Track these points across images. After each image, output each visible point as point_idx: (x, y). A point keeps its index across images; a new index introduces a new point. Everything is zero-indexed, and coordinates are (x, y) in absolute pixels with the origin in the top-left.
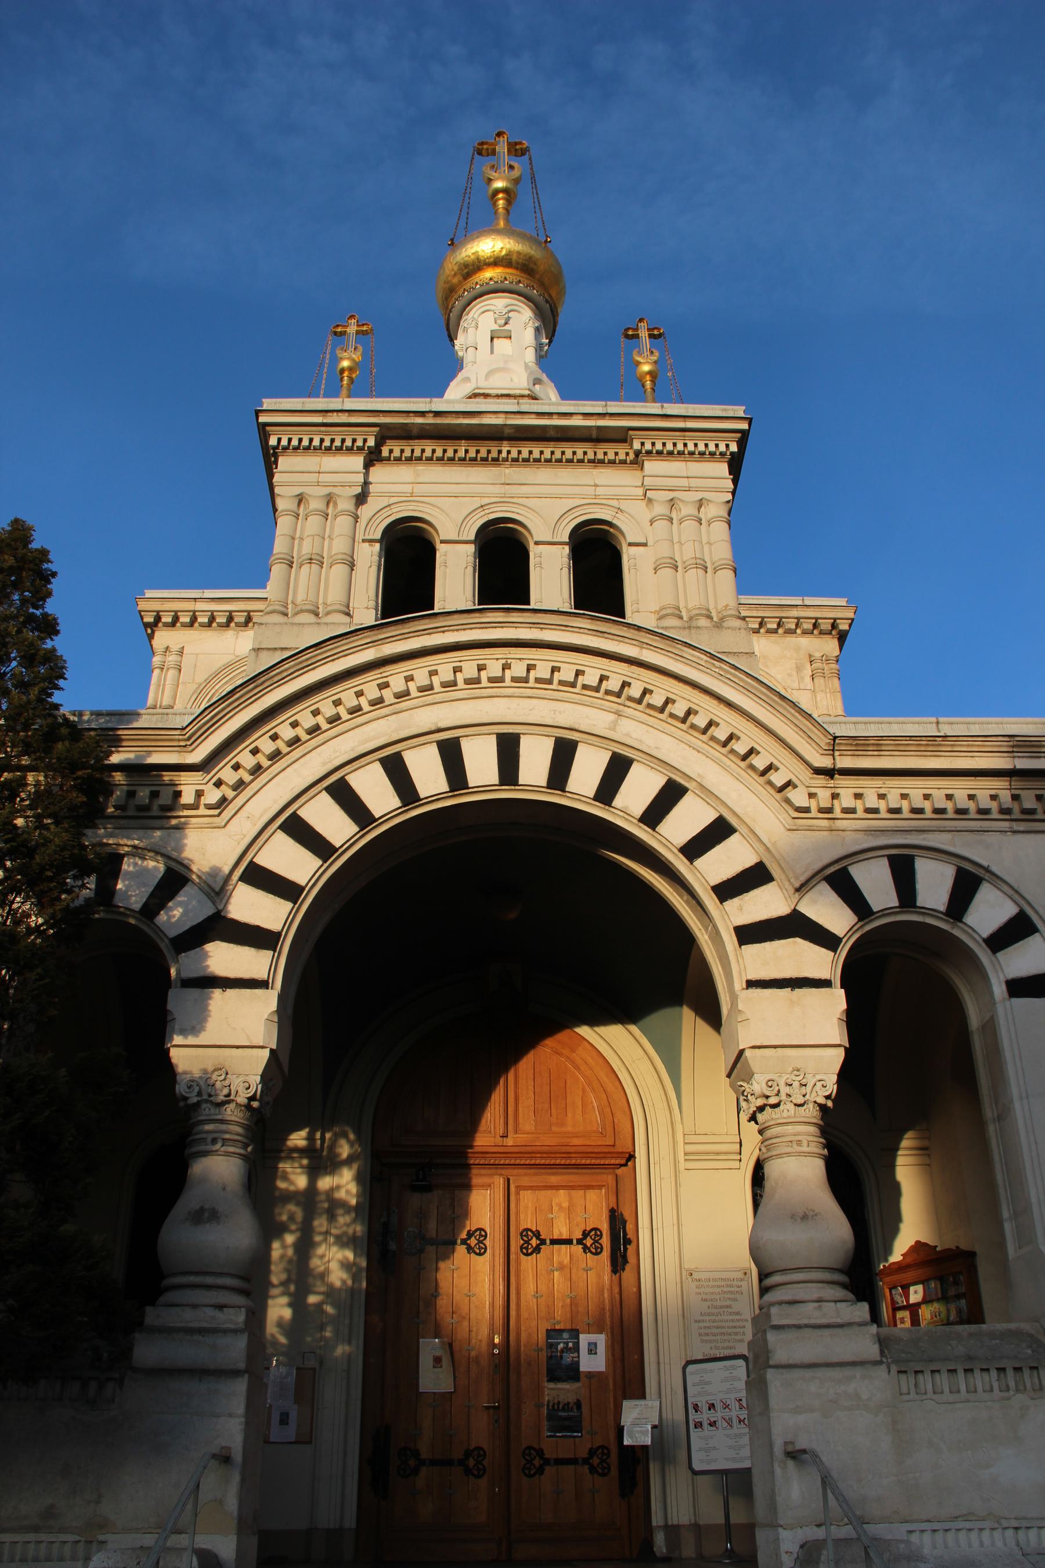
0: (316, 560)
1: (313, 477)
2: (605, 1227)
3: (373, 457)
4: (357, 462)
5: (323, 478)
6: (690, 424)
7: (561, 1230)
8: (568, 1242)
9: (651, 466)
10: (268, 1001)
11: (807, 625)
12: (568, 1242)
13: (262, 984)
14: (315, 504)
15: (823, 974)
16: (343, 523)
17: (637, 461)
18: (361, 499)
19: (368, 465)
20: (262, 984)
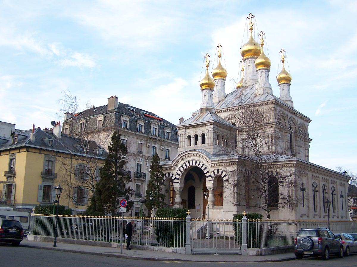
0: (182, 142)
1: (181, 133)
2: (220, 194)
3: (185, 129)
4: (184, 130)
5: (182, 132)
6: (209, 122)
7: (217, 194)
8: (217, 195)
9: (207, 127)
10: (179, 184)
11: (269, 103)
12: (217, 195)
13: (178, 183)
14: (182, 135)
15: (212, 180)
16: (184, 137)
17: (205, 126)
18: (185, 134)
19: (185, 130)
20: (178, 183)
